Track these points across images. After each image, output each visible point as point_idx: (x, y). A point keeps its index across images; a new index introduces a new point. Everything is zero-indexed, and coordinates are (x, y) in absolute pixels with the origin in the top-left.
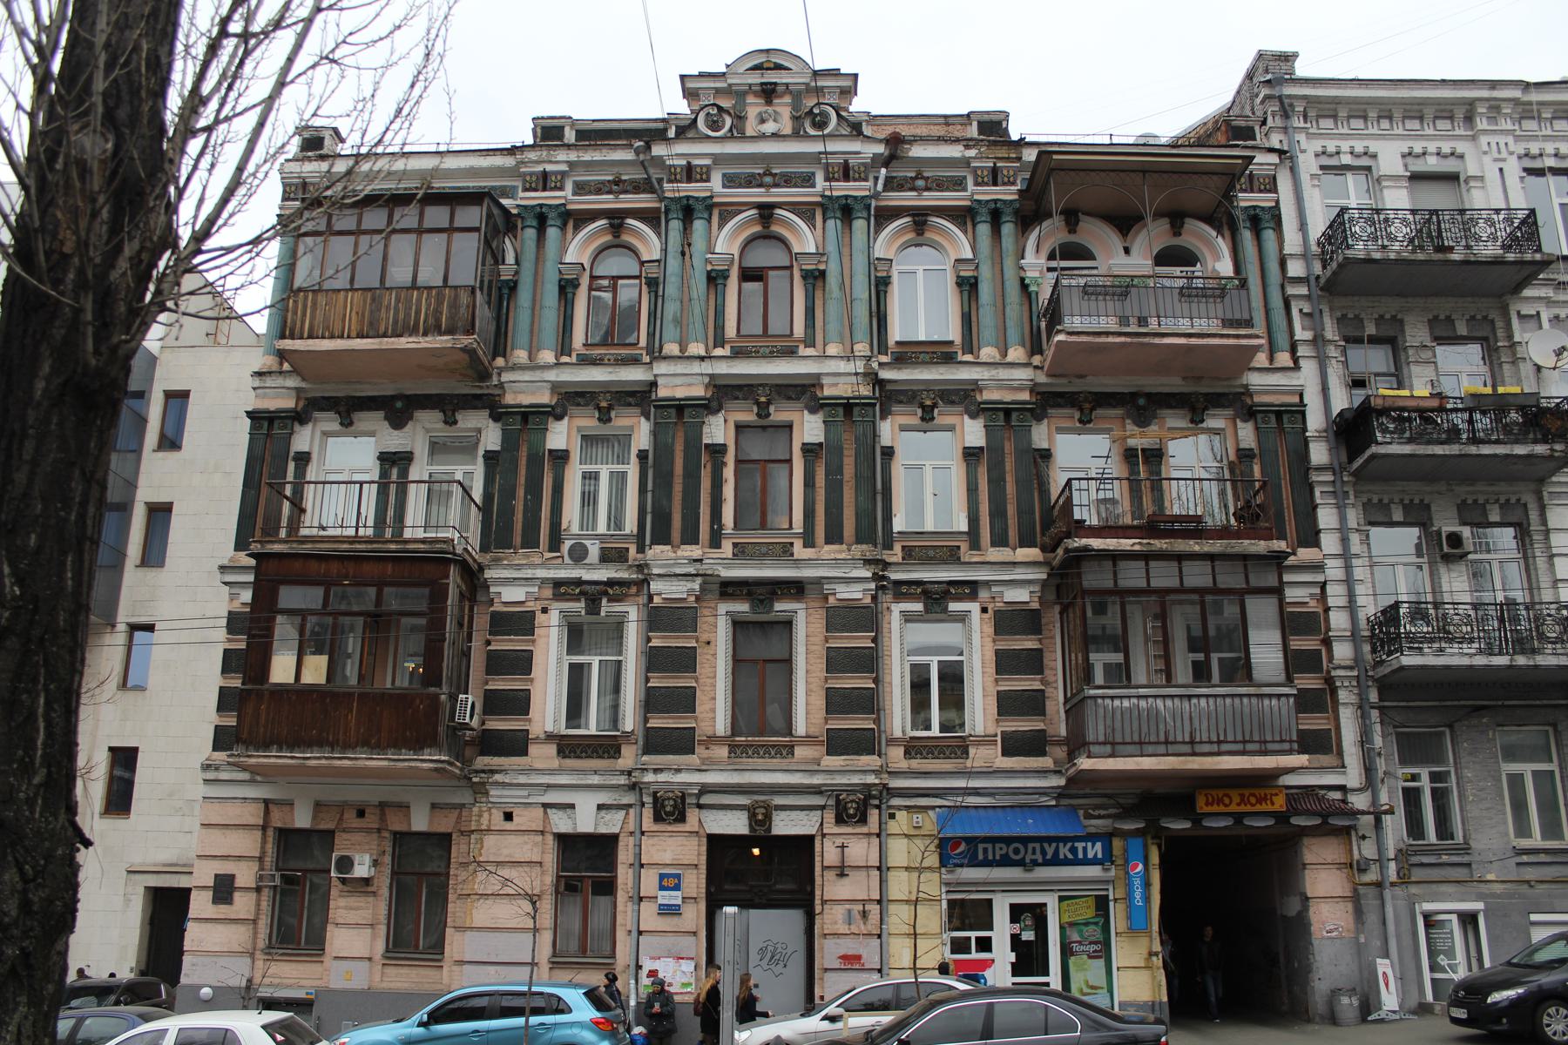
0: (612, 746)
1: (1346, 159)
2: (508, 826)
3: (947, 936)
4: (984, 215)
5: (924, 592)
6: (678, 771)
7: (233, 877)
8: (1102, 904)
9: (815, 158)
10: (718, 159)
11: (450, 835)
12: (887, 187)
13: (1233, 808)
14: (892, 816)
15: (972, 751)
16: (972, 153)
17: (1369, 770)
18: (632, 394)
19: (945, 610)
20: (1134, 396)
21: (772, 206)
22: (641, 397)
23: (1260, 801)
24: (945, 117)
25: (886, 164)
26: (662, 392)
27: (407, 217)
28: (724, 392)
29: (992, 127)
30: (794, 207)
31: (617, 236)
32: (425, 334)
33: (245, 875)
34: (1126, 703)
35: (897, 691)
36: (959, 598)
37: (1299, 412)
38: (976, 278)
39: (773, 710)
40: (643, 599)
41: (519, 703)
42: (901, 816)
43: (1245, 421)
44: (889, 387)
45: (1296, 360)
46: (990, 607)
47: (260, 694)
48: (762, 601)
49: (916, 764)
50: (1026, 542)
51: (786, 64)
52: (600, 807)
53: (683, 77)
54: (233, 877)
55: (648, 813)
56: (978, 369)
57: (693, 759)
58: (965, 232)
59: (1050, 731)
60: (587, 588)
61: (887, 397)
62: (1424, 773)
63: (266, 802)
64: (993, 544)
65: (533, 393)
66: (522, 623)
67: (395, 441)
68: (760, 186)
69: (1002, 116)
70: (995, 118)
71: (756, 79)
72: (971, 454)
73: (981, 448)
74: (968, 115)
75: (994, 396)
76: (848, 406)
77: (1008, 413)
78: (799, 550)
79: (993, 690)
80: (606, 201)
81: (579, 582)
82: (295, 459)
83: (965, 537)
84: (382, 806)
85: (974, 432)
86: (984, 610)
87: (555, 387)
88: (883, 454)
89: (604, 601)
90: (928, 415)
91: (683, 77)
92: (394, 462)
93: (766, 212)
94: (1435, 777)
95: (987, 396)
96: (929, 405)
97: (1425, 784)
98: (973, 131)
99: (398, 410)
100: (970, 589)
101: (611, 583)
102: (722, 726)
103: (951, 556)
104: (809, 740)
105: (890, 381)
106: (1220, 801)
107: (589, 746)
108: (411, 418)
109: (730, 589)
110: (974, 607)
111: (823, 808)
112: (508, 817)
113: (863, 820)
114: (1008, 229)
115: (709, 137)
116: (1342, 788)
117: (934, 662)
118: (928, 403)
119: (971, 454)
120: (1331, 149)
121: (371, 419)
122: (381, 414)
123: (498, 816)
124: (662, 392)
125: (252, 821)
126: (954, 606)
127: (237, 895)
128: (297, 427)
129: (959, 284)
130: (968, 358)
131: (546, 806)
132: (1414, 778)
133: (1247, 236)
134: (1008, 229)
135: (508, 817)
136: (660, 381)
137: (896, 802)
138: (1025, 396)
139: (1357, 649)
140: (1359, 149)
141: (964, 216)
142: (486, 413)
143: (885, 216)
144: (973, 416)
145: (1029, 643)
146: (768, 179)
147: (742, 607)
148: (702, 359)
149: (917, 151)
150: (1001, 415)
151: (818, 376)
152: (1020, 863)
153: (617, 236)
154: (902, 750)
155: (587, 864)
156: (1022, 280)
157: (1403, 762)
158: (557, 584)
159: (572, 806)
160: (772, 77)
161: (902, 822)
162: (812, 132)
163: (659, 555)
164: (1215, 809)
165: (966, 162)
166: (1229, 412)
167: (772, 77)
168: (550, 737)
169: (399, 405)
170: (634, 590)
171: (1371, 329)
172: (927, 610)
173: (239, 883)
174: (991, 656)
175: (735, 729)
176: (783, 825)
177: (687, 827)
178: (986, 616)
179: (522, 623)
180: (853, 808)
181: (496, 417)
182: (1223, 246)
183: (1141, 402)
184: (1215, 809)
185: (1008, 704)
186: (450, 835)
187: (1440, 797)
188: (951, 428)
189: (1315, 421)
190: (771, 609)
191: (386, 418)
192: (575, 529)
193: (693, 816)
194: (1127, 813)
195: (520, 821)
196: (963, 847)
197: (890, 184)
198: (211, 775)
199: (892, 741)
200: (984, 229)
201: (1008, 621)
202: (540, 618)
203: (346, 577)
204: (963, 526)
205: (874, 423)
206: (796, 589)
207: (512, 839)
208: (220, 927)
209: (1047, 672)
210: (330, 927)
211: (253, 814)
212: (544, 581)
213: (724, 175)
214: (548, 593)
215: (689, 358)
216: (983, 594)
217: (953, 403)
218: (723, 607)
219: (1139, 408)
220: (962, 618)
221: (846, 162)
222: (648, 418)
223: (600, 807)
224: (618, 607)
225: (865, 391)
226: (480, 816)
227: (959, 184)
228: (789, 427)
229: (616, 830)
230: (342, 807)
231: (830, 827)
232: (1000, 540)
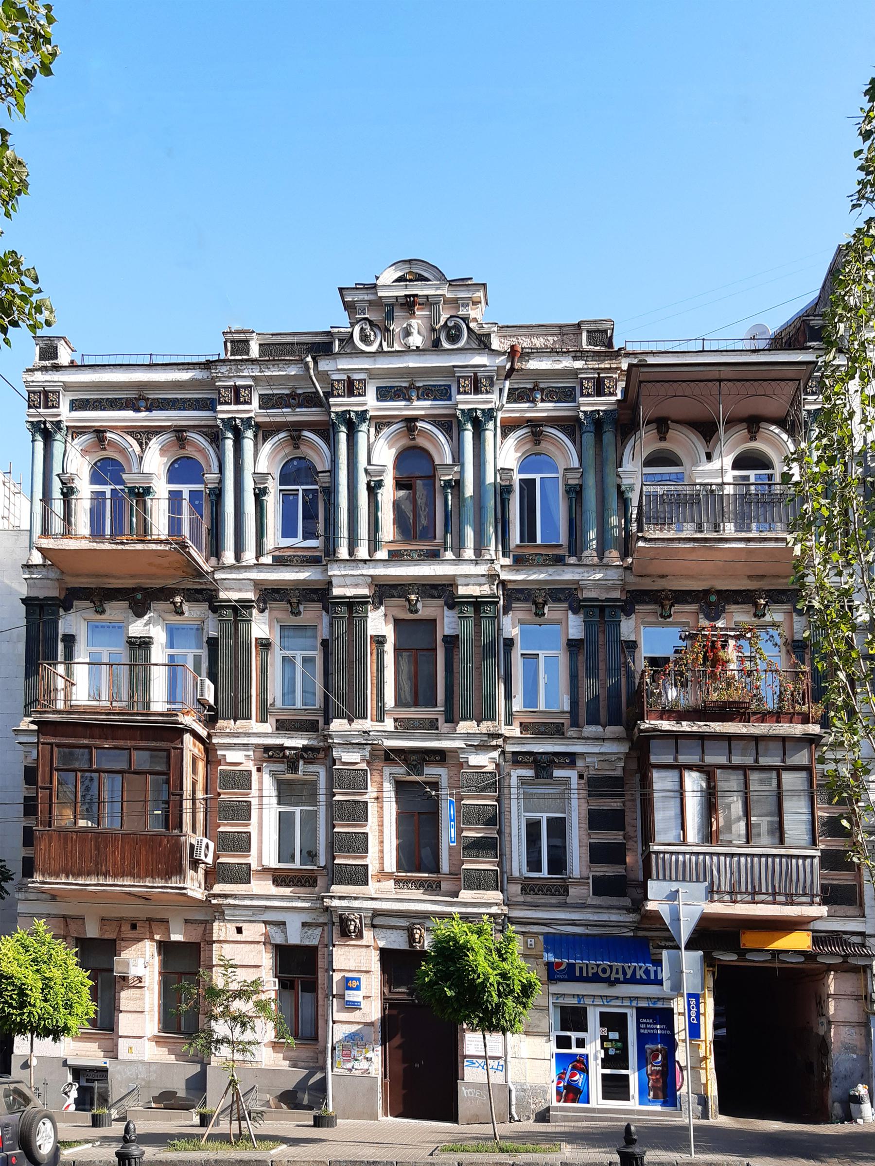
0: (311, 877)
5: (535, 761)
10: (372, 374)
11: (199, 943)
15: (571, 890)
19: (551, 776)
20: (707, 592)
21: (415, 419)
24: (560, 327)
26: (336, 591)
28: (385, 591)
35: (515, 840)
36: (562, 766)
38: (581, 486)
40: (328, 762)
41: (242, 843)
44: (510, 586)
46: (585, 774)
48: (415, 766)
50: (613, 721)
51: (426, 275)
52: (304, 924)
53: (341, 290)
55: (336, 930)
56: (580, 570)
58: (574, 442)
59: (631, 876)
60: (287, 752)
65: (240, 590)
69: (608, 325)
72: (573, 646)
73: (581, 640)
74: (579, 325)
76: (477, 604)
77: (602, 609)
78: (444, 727)
79: (586, 841)
81: (282, 748)
82: (62, 640)
83: (568, 716)
85: (575, 626)
86: (581, 777)
87: (256, 583)
88: (505, 645)
89: (301, 762)
91: (341, 290)
95: (587, 594)
100: (569, 760)
101: (305, 749)
105: (510, 581)
107: (295, 877)
109: (391, 756)
110: (573, 774)
114: (609, 437)
115: (363, 352)
117: (544, 817)
118: (541, 601)
119: (573, 646)
126: (557, 773)
129: (567, 492)
130: (573, 560)
134: (609, 437)
136: (335, 581)
141: (571, 426)
144: (575, 612)
145: (615, 804)
147: (400, 771)
148: (365, 561)
149: (533, 364)
150: (597, 611)
154: (520, 887)
156: (619, 486)
158: (267, 748)
159: (284, 923)
162: (446, 345)
163: (338, 725)
170: (322, 755)
172: (537, 776)
174: (585, 814)
177: (363, 942)
178: (582, 781)
179: (242, 780)
183: (713, 598)
185: (598, 854)
186: (199, 943)
188: (558, 622)
190: (420, 773)
192: (279, 704)
199: (511, 880)
200: (588, 439)
201: (597, 786)
204: (567, 708)
205: (497, 617)
209: (628, 829)
212: (257, 746)
213: (378, 388)
215: (354, 561)
216: (580, 763)
217: (559, 600)
218: (387, 770)
219: (710, 604)
220: (566, 781)
221: (475, 374)
222: (327, 612)
224: (312, 768)
232: (593, 720)
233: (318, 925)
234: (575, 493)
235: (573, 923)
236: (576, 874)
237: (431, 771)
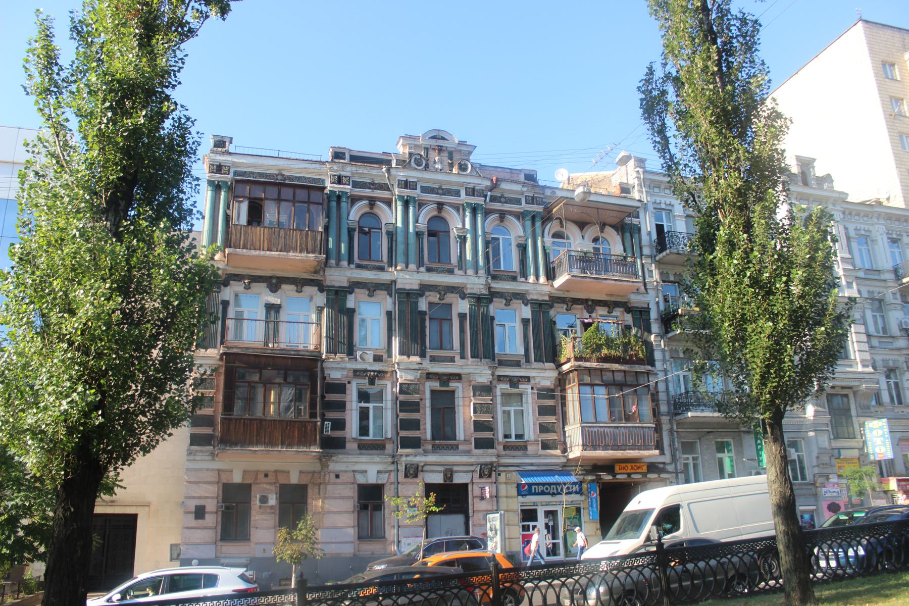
1: (663, 206)
2: (338, 480)
3: (521, 524)
4: (529, 217)
6: (416, 456)
7: (203, 507)
8: (578, 510)
9: (462, 184)
12: (491, 201)
13: (629, 471)
14: (499, 475)
15: (529, 448)
16: (525, 189)
17: (673, 456)
18: (383, 284)
20: (587, 300)
22: (388, 287)
23: (638, 468)
25: (491, 191)
27: (287, 193)
28: (425, 288)
29: (531, 178)
30: (450, 205)
31: (371, 208)
32: (301, 252)
33: (211, 506)
34: (596, 429)
37: (647, 311)
39: (448, 429)
42: (503, 474)
43: (628, 313)
45: (646, 289)
47: (230, 420)
49: (507, 452)
52: (379, 472)
54: (203, 507)
57: (420, 450)
61: (492, 295)
62: (690, 457)
63: (219, 470)
64: (536, 361)
66: (341, 388)
67: (274, 299)
68: (437, 194)
70: (532, 173)
71: (434, 143)
72: (525, 322)
75: (535, 297)
77: (540, 304)
80: (368, 192)
84: (276, 472)
86: (532, 388)
90: (507, 304)
92: (272, 309)
93: (440, 206)
94: (694, 459)
96: (510, 298)
97: (691, 462)
98: (522, 178)
99: (274, 283)
102: (429, 436)
103: (517, 364)
104: (466, 441)
106: (624, 468)
108: (280, 287)
109: (429, 376)
110: (529, 387)
111: (473, 471)
112: (337, 476)
113: (490, 476)
114: (538, 224)
116: (664, 463)
119: (525, 322)
120: (658, 201)
121: (261, 288)
122: (265, 285)
123: (333, 476)
124: (399, 286)
125: (212, 479)
127: (207, 516)
128: (222, 287)
131: (354, 471)
132: (688, 459)
133: (628, 235)
134: (538, 224)
135: (337, 476)
137: (501, 469)
138: (547, 298)
139: (669, 408)
140: (668, 202)
141: (520, 216)
142: (316, 288)
143: (487, 213)
146: (440, 191)
147: (436, 385)
151: (466, 284)
152: (549, 494)
153: (371, 208)
155: (370, 498)
157: (684, 453)
159: (366, 472)
160: (441, 143)
161: (502, 478)
164: (622, 471)
165: (522, 193)
166: (622, 309)
167: (441, 143)
168: (355, 439)
169: (274, 281)
171: (672, 278)
173: (208, 509)
175: (433, 438)
176: (459, 479)
180: (488, 471)
181: (321, 290)
182: (618, 239)
183: (590, 303)
184: (622, 471)
187: (695, 466)
189: (653, 315)
190: (448, 386)
191: (268, 287)
193: (420, 475)
194: (588, 472)
195: (343, 478)
196: (526, 487)
197: (493, 199)
198: (191, 457)
200: (528, 223)
202: (348, 386)
203: (269, 366)
204: (523, 353)
206: (458, 377)
207: (340, 487)
208: (199, 531)
210: (252, 529)
211: (213, 477)
214: (351, 374)
216: (532, 381)
219: (588, 306)
223: (379, 472)
224: (382, 382)
225: (485, 292)
226: (325, 476)
227: (518, 202)
228: (450, 306)
229: (384, 482)
230: (257, 473)
231: (476, 479)
233: (386, 472)
234: (523, 248)
235: (532, 465)
236: (532, 438)
237: (453, 385)
